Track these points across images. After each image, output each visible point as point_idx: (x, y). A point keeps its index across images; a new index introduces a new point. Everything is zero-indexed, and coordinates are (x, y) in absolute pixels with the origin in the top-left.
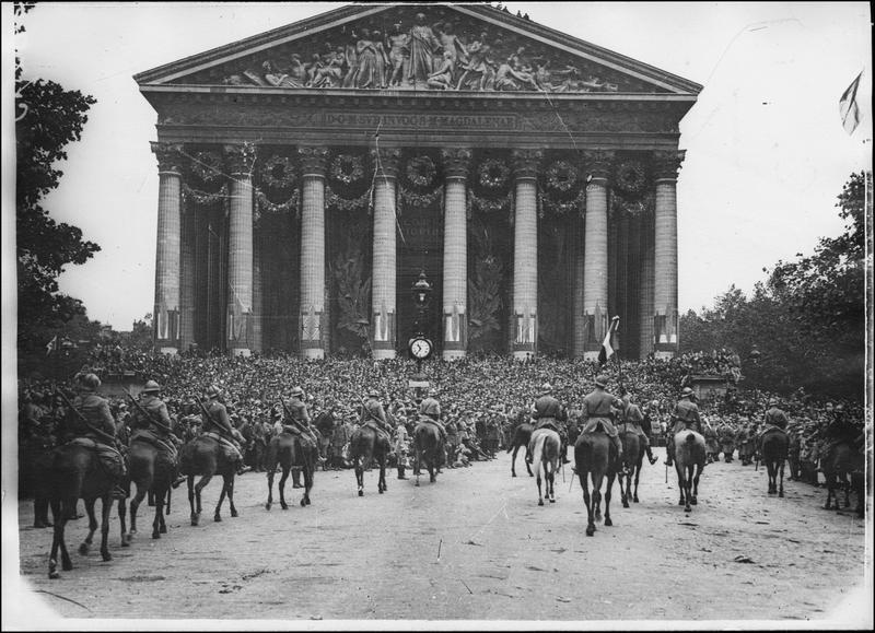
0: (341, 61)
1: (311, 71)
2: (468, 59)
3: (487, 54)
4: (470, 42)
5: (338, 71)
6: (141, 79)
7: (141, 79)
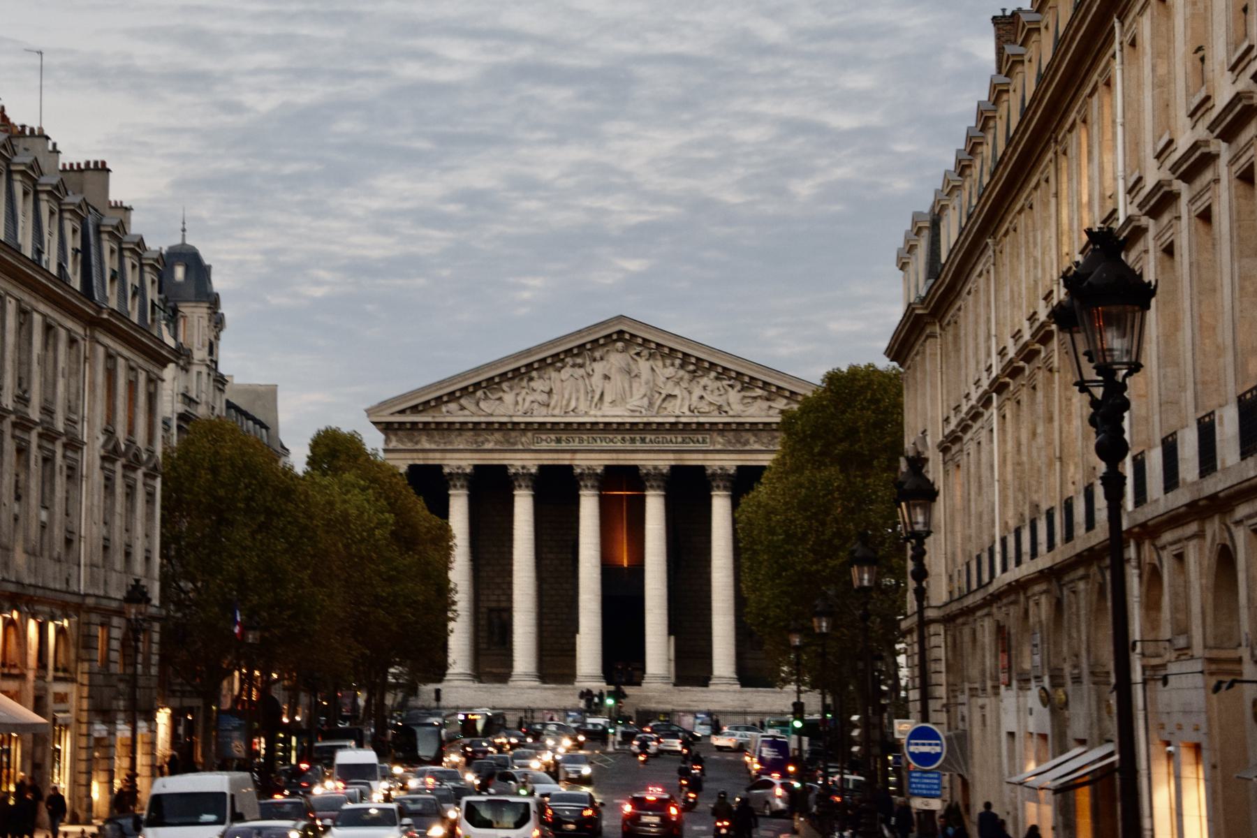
0: (547, 389)
1: (520, 399)
2: (665, 384)
3: (681, 379)
4: (665, 366)
5: (545, 397)
6: (369, 412)
7: (369, 412)
